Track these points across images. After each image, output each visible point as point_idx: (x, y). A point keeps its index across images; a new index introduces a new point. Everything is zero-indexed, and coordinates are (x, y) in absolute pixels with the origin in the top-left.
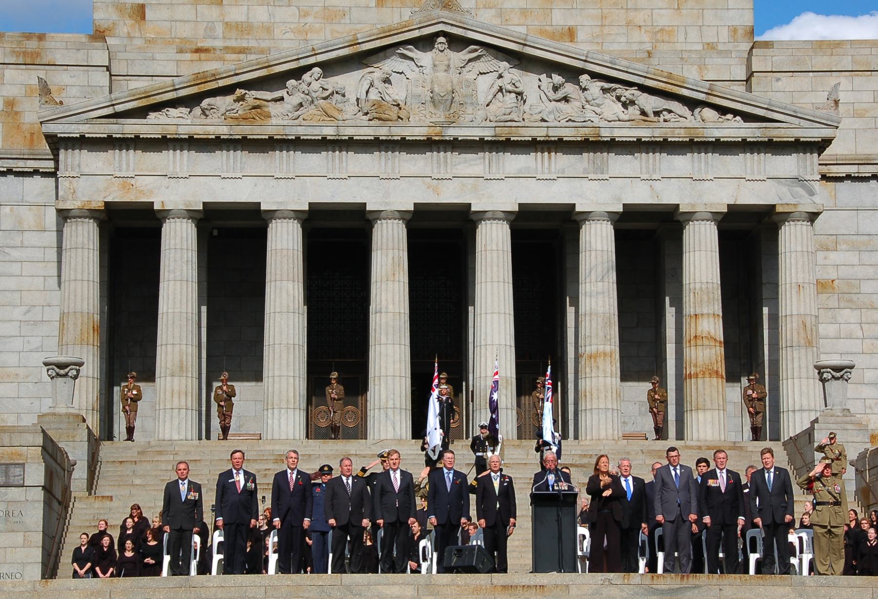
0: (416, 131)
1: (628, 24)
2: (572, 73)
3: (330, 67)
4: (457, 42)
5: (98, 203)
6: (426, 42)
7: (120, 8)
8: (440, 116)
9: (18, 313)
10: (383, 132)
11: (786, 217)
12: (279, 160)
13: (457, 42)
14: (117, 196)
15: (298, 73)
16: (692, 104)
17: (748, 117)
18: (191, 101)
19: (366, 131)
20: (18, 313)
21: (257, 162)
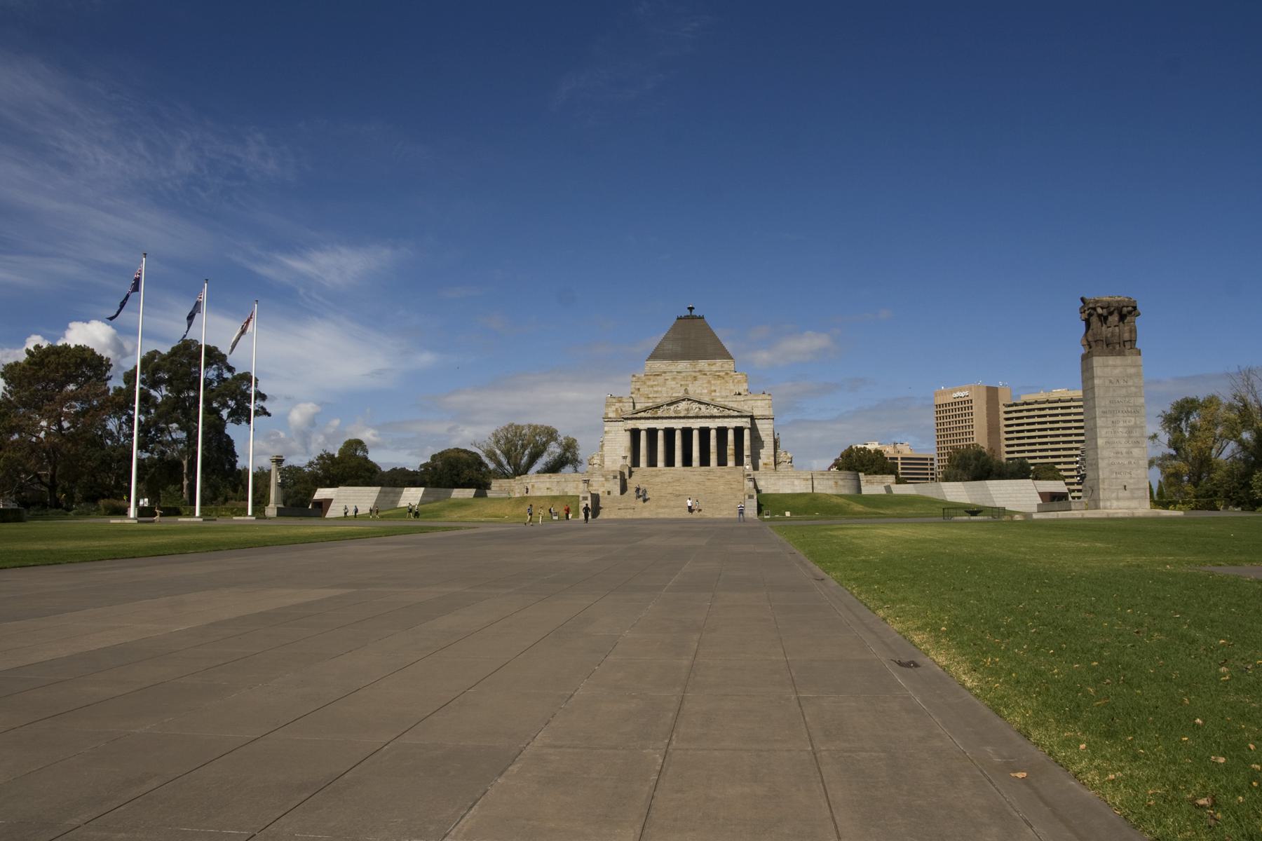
0: (682, 415)
1: (726, 389)
2: (708, 405)
3: (668, 405)
4: (689, 400)
5: (630, 428)
6: (684, 400)
7: (635, 388)
8: (686, 412)
9: (618, 445)
10: (677, 415)
11: (746, 428)
12: (660, 421)
13: (689, 400)
14: (633, 427)
15: (662, 406)
16: (729, 409)
17: (738, 412)
18: (645, 411)
19: (674, 415)
20: (618, 445)
21: (656, 421)
